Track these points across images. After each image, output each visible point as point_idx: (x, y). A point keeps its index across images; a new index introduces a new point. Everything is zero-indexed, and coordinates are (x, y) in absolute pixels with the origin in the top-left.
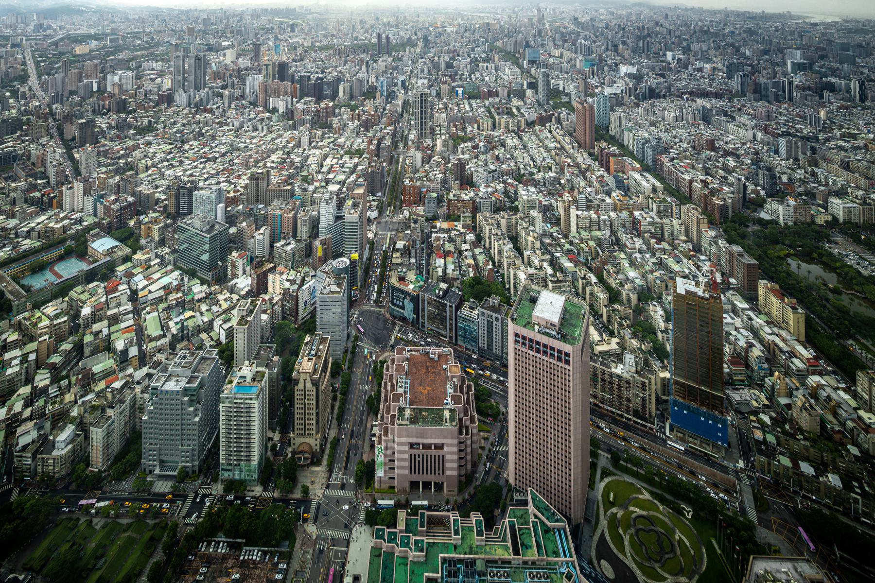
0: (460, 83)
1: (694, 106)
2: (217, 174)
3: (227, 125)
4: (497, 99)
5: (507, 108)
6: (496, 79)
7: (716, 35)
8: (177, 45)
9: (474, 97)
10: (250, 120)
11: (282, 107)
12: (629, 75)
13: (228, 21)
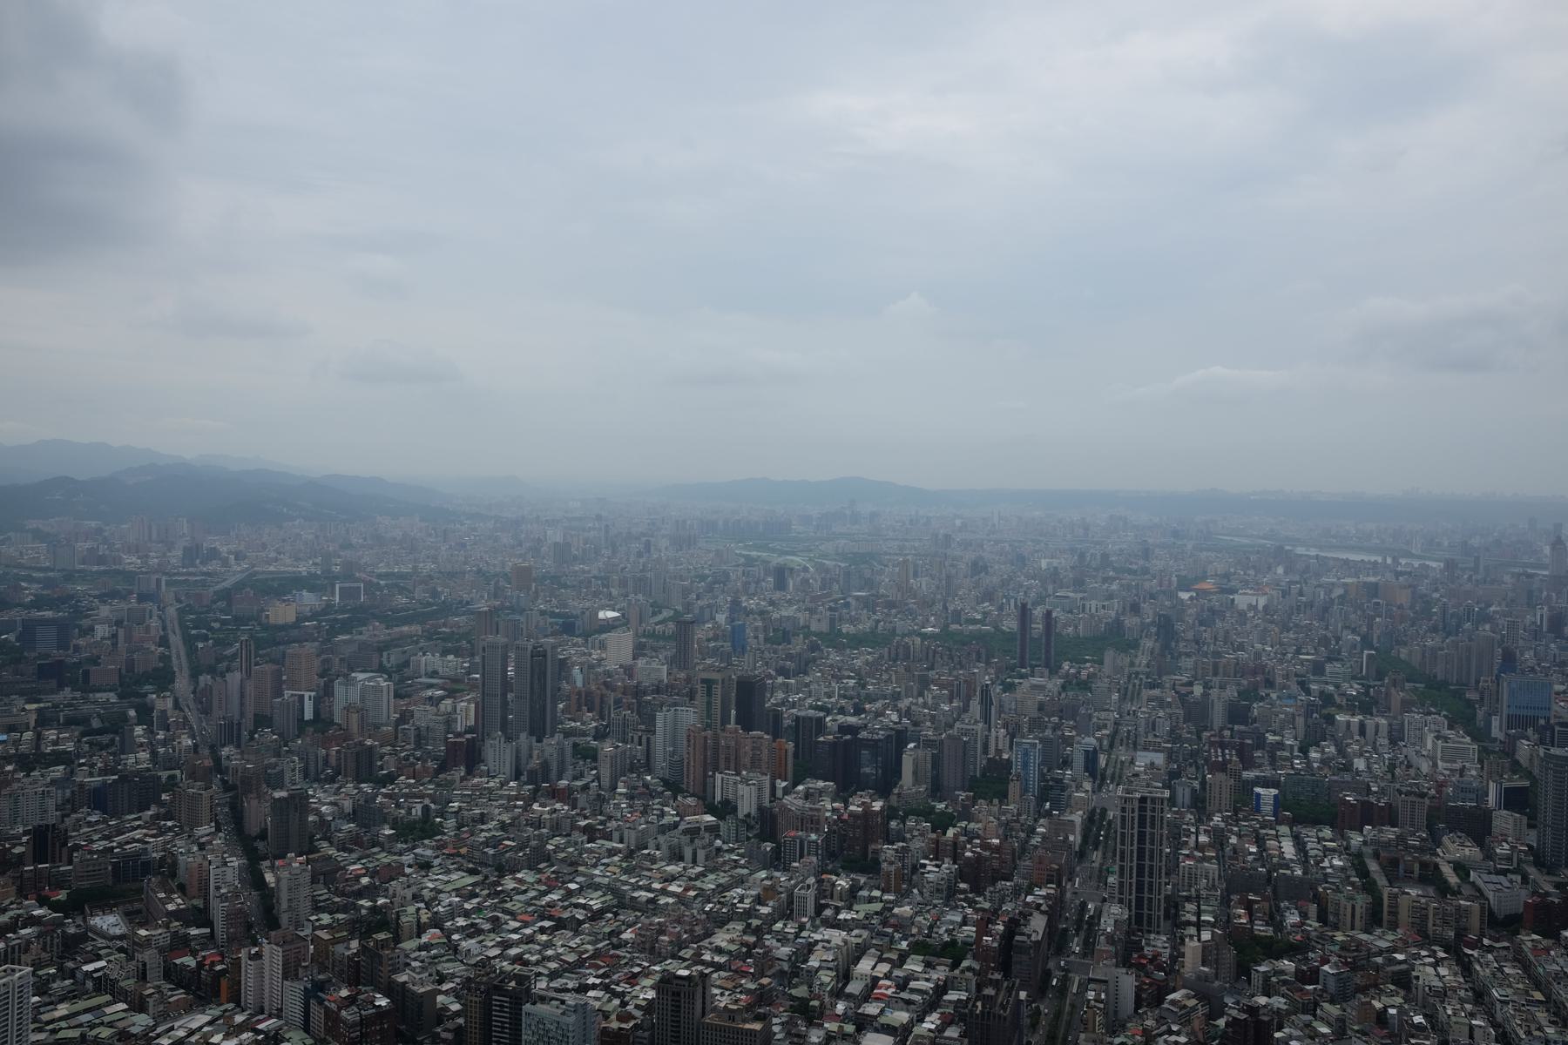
0: (1268, 772)
4: (1390, 833)
5: (1424, 865)
6: (1392, 767)
9: (1316, 822)
10: (663, 830)
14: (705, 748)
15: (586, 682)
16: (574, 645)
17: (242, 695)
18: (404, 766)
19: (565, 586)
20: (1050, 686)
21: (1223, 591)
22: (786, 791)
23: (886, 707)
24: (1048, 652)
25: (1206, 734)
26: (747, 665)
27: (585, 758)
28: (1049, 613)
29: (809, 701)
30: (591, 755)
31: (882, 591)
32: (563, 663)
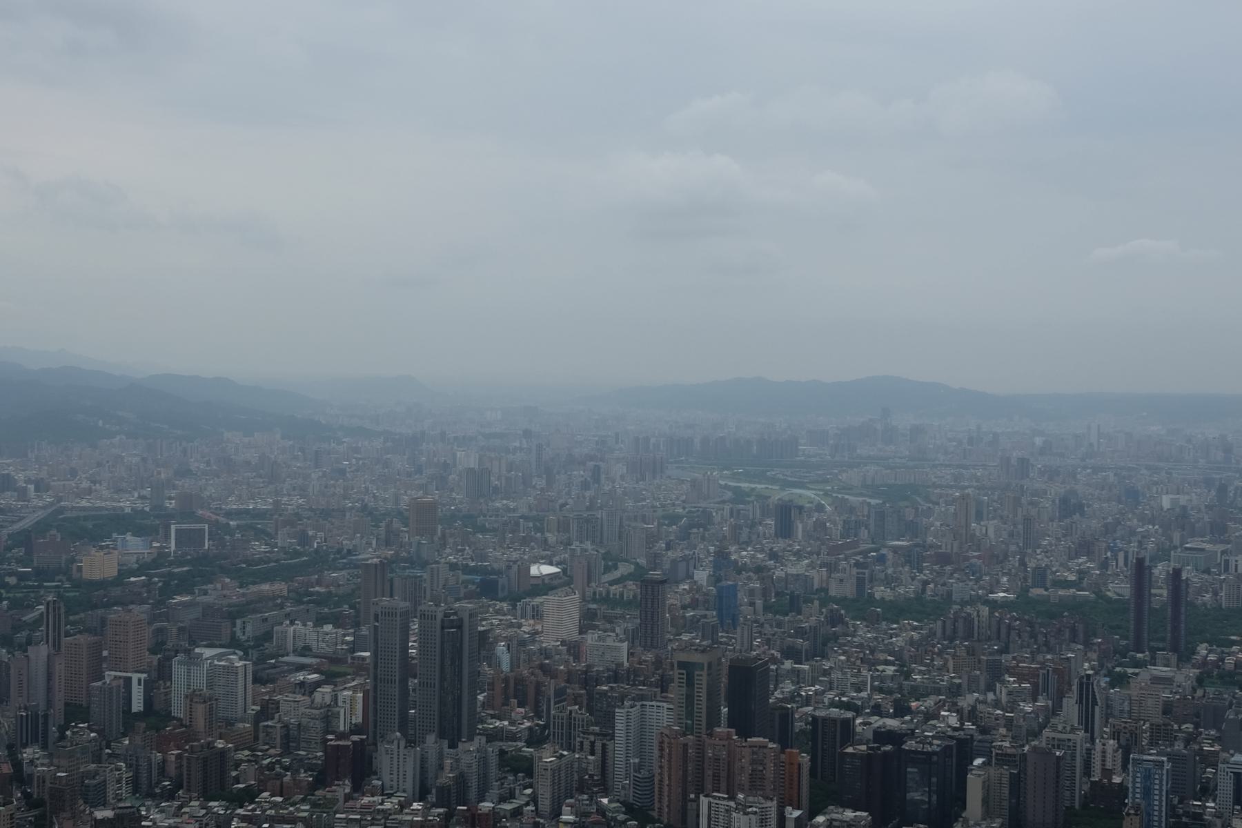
8: (384, 566)
15: (514, 664)
16: (498, 612)
17: (49, 676)
18: (268, 779)
20: (1179, 678)
23: (940, 705)
24: (1175, 629)
26: (738, 644)
27: (515, 771)
28: (1177, 573)
29: (830, 695)
30: (526, 768)
31: (930, 539)
32: (483, 636)
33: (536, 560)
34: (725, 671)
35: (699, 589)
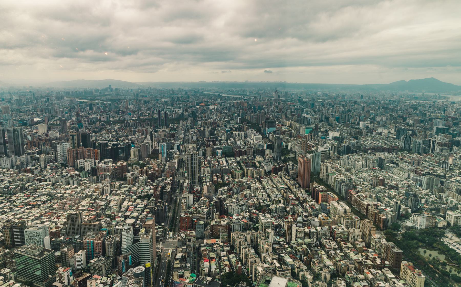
1: (375, 157)
2: (41, 216)
3: (46, 181)
4: (245, 157)
5: (252, 163)
6: (245, 143)
7: (392, 110)
11: (88, 166)
12: (335, 138)
13: (37, 101)
14: (74, 154)
15: (32, 139)
19: (22, 112)
20: (167, 130)
21: (206, 105)
22: (99, 163)
25: (205, 139)
27: (35, 160)
28: (166, 112)
30: (38, 159)
33: (35, 118)
34: (81, 136)
35: (74, 121)
